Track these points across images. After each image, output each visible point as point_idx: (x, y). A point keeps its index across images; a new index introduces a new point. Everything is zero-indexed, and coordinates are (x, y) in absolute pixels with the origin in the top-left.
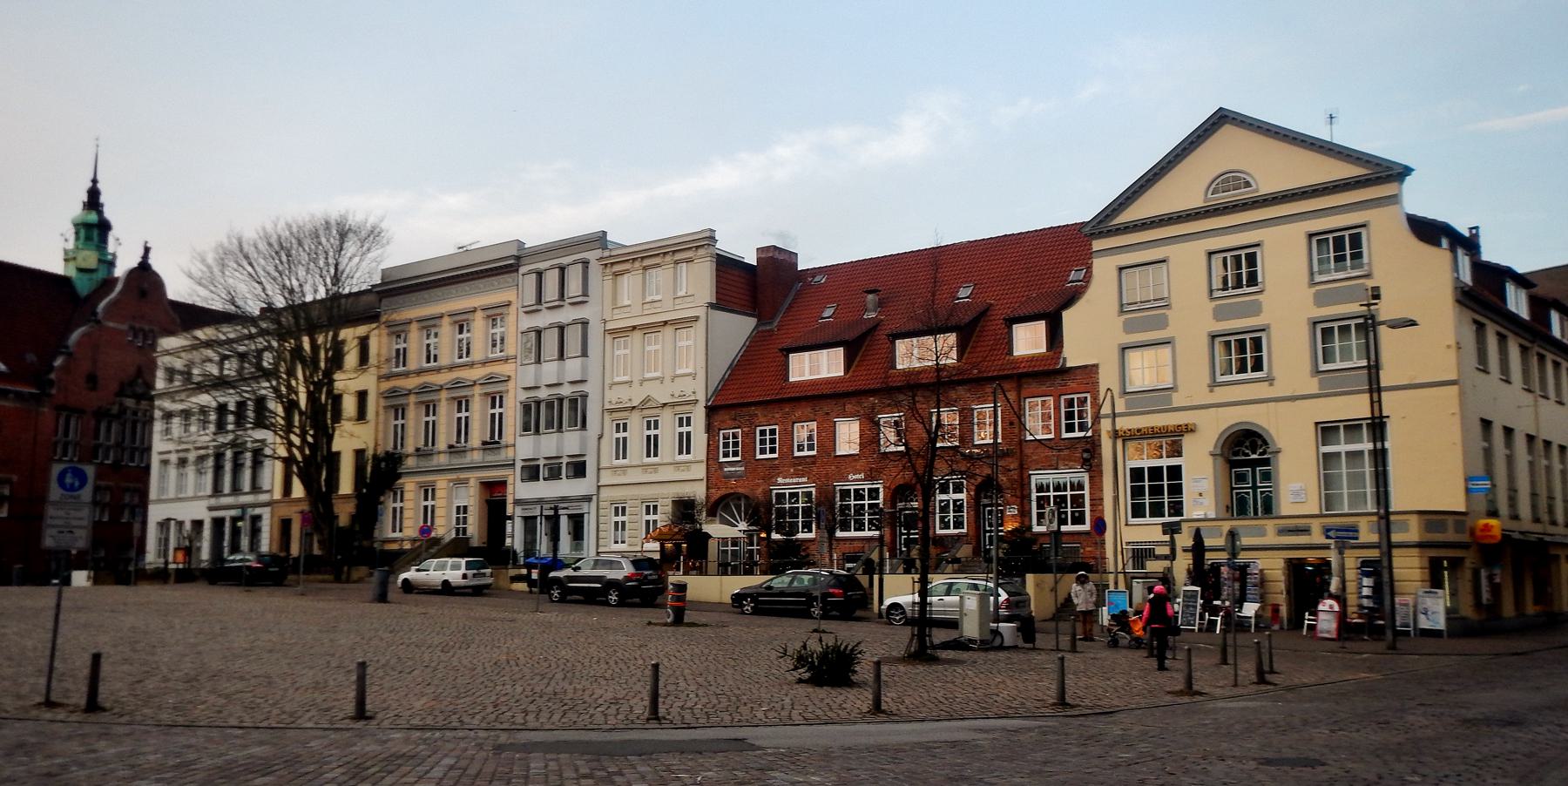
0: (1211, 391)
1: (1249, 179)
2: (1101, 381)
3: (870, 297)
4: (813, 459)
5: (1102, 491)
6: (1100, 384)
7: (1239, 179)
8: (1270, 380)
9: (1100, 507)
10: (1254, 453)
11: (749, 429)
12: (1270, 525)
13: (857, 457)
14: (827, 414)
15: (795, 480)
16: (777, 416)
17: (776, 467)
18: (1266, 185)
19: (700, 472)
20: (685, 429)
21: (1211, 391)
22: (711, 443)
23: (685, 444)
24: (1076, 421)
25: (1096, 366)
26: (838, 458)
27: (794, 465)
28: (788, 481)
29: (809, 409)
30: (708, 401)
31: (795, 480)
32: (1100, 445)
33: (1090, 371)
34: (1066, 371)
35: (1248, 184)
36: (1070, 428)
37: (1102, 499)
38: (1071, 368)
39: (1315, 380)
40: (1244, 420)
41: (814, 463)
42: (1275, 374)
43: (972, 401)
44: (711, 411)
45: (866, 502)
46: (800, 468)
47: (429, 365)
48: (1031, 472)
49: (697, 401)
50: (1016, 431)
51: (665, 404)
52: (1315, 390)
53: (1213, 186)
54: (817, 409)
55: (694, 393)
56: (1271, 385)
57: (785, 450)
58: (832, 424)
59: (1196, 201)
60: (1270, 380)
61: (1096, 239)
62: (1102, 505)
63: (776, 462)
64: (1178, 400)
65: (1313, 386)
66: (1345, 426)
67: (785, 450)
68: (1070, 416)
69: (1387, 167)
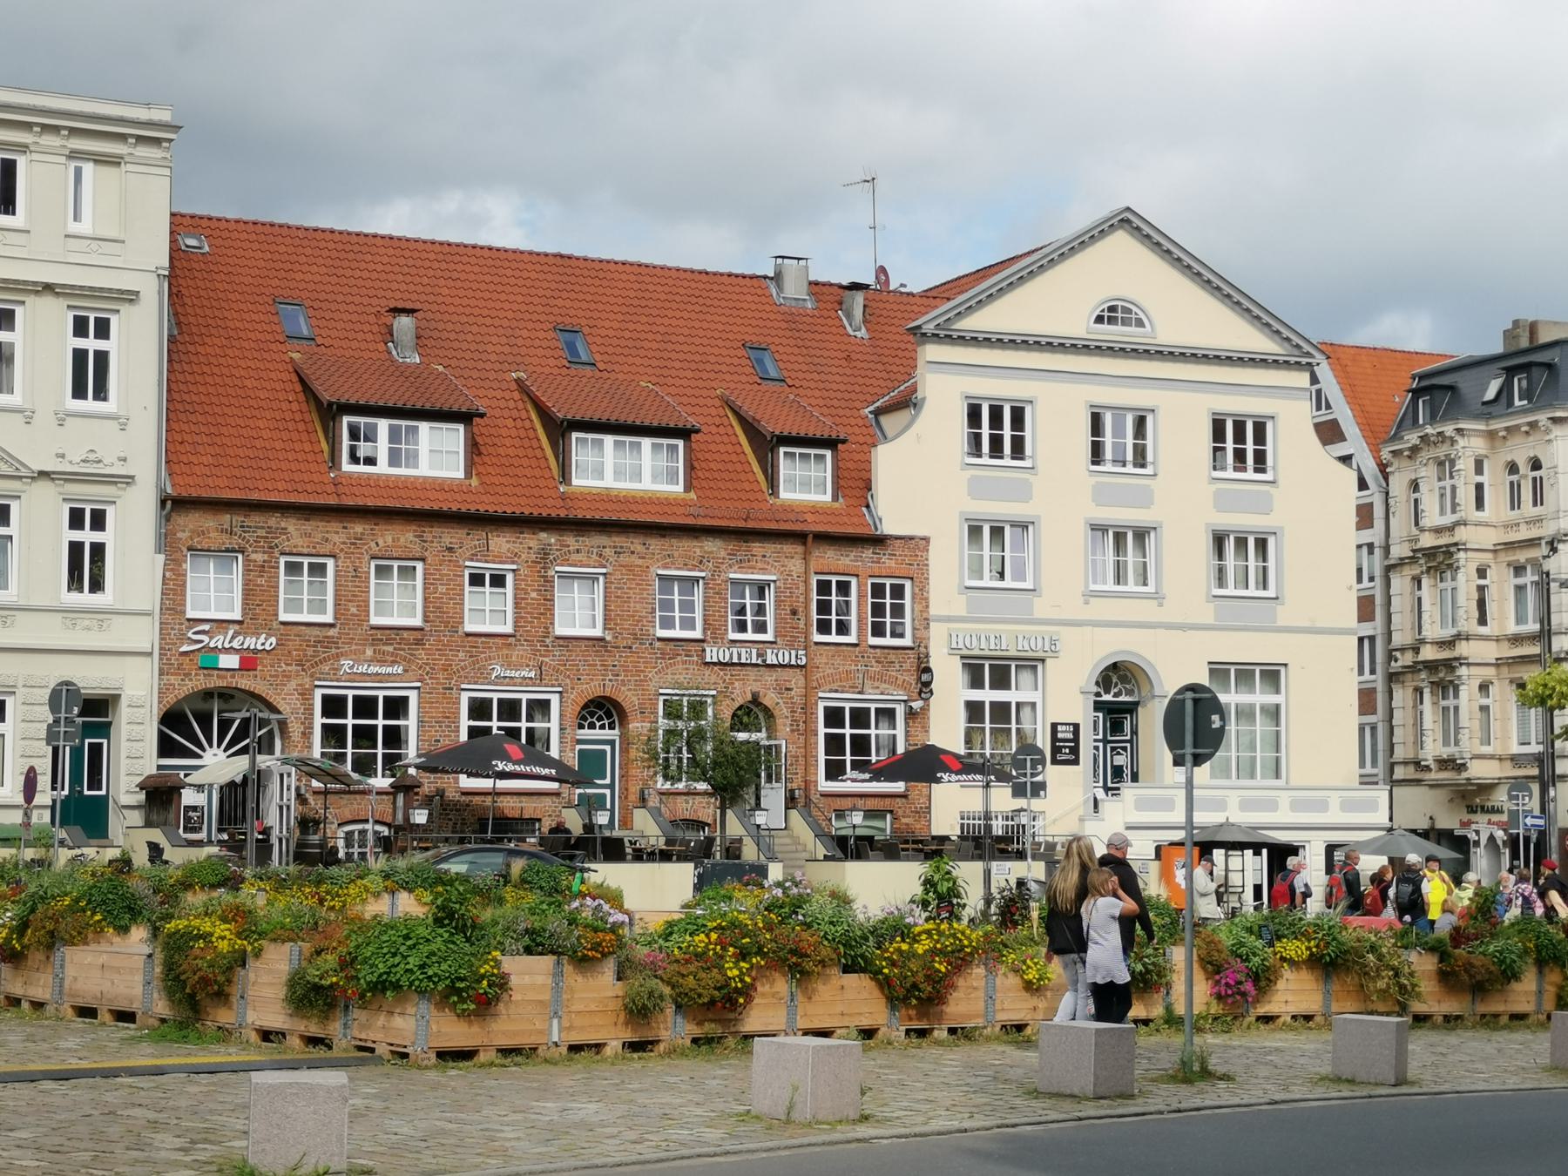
0: (1087, 603)
1: (1142, 316)
2: (931, 562)
3: (404, 323)
4: (418, 635)
5: (927, 731)
6: (930, 568)
7: (1130, 311)
8: (1157, 597)
10: (1107, 691)
11: (266, 557)
12: (1284, 798)
13: (511, 640)
14: (450, 549)
15: (374, 669)
16: (336, 538)
17: (328, 643)
18: (1166, 334)
19: (145, 634)
20: (87, 536)
21: (1087, 603)
22: (168, 574)
24: (834, 617)
25: (926, 539)
26: (470, 638)
27: (375, 642)
28: (362, 669)
29: (410, 536)
31: (374, 669)
33: (917, 545)
34: (879, 541)
35: (1140, 323)
36: (878, 630)
39: (1212, 605)
40: (1112, 650)
41: (419, 642)
42: (1165, 590)
44: (174, 505)
46: (390, 649)
47: (1479, 514)
48: (821, 695)
49: (129, 480)
50: (802, 622)
51: (43, 474)
52: (1209, 619)
53: (1097, 312)
54: (429, 537)
55: (125, 460)
56: (1161, 605)
57: (354, 610)
59: (1079, 326)
60: (1157, 597)
61: (934, 343)
63: (332, 632)
64: (1042, 607)
65: (1207, 615)
66: (1261, 671)
67: (354, 610)
68: (878, 610)
69: (1308, 353)
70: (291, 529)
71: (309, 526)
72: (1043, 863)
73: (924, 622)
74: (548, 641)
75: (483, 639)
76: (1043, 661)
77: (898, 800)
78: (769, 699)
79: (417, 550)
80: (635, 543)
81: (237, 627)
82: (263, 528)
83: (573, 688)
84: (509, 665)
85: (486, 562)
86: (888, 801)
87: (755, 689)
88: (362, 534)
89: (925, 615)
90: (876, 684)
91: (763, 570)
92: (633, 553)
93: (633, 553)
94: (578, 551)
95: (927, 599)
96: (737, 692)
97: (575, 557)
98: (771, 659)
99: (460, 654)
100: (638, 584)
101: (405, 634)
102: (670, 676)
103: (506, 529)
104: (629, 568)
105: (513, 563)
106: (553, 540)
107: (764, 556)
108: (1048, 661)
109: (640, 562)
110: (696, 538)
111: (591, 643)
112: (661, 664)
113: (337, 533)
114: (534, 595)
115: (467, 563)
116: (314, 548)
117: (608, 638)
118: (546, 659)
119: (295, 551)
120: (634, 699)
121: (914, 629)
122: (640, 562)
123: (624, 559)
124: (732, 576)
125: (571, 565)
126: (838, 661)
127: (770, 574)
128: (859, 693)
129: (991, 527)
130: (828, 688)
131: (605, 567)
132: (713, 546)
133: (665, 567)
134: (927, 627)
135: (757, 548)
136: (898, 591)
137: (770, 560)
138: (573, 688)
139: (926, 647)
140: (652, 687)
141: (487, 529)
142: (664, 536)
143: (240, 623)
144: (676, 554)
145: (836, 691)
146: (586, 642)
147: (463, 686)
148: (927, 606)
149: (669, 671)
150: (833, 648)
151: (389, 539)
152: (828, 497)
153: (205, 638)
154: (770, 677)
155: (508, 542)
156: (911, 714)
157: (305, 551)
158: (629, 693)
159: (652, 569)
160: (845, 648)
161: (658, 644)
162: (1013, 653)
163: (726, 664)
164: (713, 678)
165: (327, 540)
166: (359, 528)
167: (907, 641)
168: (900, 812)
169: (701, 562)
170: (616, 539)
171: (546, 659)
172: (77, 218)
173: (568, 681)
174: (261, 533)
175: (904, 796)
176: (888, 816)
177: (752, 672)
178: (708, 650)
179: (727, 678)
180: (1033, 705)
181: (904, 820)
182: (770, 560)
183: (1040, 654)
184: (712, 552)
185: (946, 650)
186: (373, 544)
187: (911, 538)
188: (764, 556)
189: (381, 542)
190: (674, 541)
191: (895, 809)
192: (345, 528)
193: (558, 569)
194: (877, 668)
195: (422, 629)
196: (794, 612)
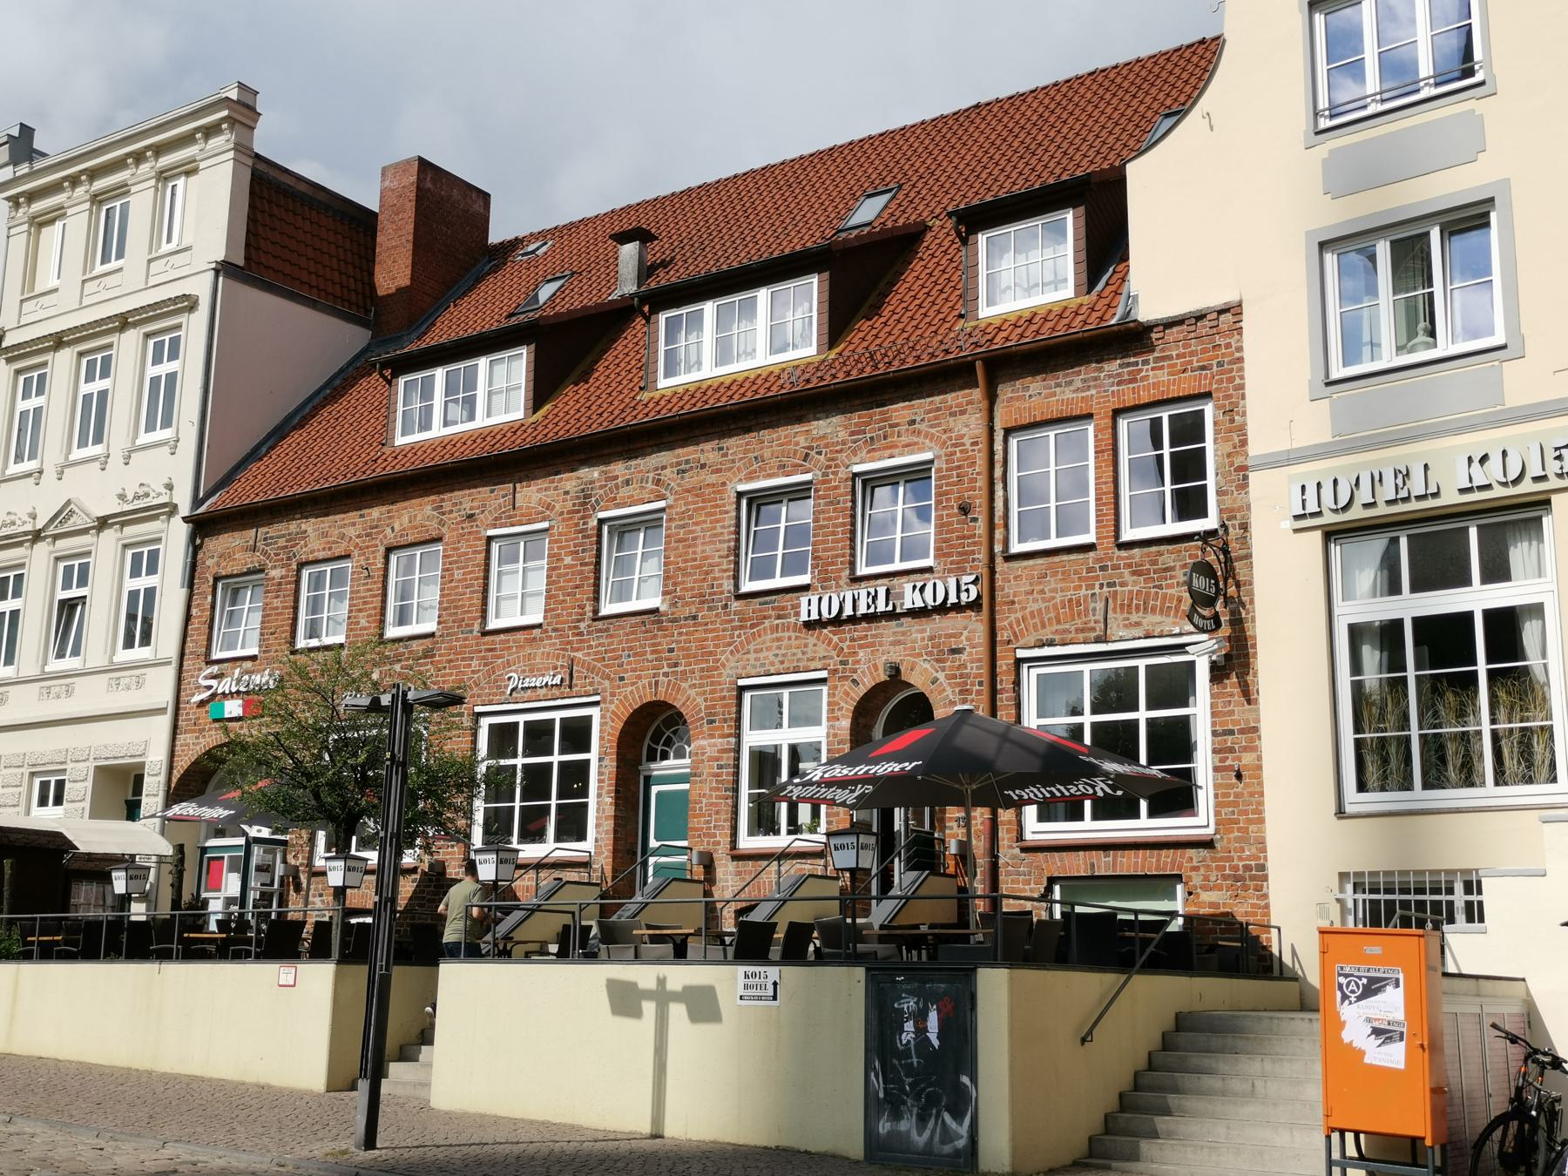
2: (1246, 354)
3: (629, 250)
6: (1246, 365)
9: (1247, 758)
11: (283, 571)
13: (536, 632)
14: (470, 516)
16: (351, 532)
23: (138, 627)
25: (1233, 310)
26: (488, 638)
30: (197, 502)
32: (1249, 556)
37: (1255, 730)
38: (1148, 328)
41: (428, 654)
43: (855, 453)
45: (556, 758)
48: (1021, 654)
57: (363, 622)
58: (482, 545)
62: (1253, 748)
67: (363, 622)
70: (310, 530)
71: (325, 523)
72: (860, 972)
73: (1239, 475)
74: (582, 625)
75: (502, 637)
76: (1548, 502)
77: (1191, 852)
78: (920, 676)
79: (433, 529)
80: (707, 452)
81: (248, 665)
82: (284, 536)
83: (613, 695)
84: (531, 671)
85: (513, 525)
86: (1167, 856)
87: (894, 657)
88: (379, 520)
89: (1238, 461)
90: (1134, 618)
91: (910, 447)
92: (703, 466)
93: (703, 466)
94: (627, 483)
95: (1242, 430)
96: (862, 667)
97: (624, 492)
98: (911, 599)
99: (475, 663)
100: (707, 515)
101: (415, 645)
102: (752, 656)
103: (537, 472)
104: (696, 491)
105: (544, 519)
106: (596, 474)
107: (913, 422)
108: (1555, 498)
109: (712, 478)
110: (800, 420)
111: (638, 619)
112: (740, 637)
113: (354, 524)
114: (568, 560)
115: (491, 532)
116: (330, 549)
117: (663, 608)
118: (579, 655)
119: (311, 557)
120: (700, 700)
121: (1219, 493)
122: (712, 478)
123: (691, 480)
124: (857, 469)
125: (618, 506)
126: (1052, 583)
127: (922, 450)
128: (1098, 640)
129: (1395, 244)
130: (1032, 640)
131: (663, 498)
132: (830, 427)
133: (750, 478)
134: (1244, 485)
135: (900, 411)
136: (1189, 429)
137: (923, 427)
138: (613, 695)
139: (1245, 527)
140: (726, 675)
141: (517, 476)
142: (748, 430)
143: (253, 658)
144: (767, 453)
145: (1051, 644)
146: (634, 620)
147: (478, 709)
148: (1244, 443)
149: (752, 647)
150: (1039, 561)
151: (406, 519)
152: (1067, 292)
153: (214, 683)
154: (919, 632)
155: (539, 491)
156: (1218, 673)
157: (321, 555)
158: (692, 692)
159: (729, 486)
160: (1065, 557)
161: (735, 605)
162: (1450, 498)
163: (837, 621)
164: (822, 650)
165: (343, 536)
166: (375, 513)
167: (1210, 523)
168: (1197, 879)
169: (807, 455)
170: (680, 451)
171: (579, 655)
172: (169, 240)
173: (607, 683)
174: (282, 542)
175: (1208, 844)
176: (1179, 888)
177: (888, 629)
178: (804, 600)
179: (844, 645)
180: (1537, 610)
181: (1206, 897)
182: (923, 427)
183: (1527, 487)
184: (824, 437)
185: (1288, 524)
186: (389, 530)
187: (1200, 317)
188: (913, 422)
189: (397, 527)
190: (765, 434)
191: (1185, 874)
192: (362, 516)
193: (602, 515)
194: (1134, 585)
195: (432, 635)
196: (965, 510)
